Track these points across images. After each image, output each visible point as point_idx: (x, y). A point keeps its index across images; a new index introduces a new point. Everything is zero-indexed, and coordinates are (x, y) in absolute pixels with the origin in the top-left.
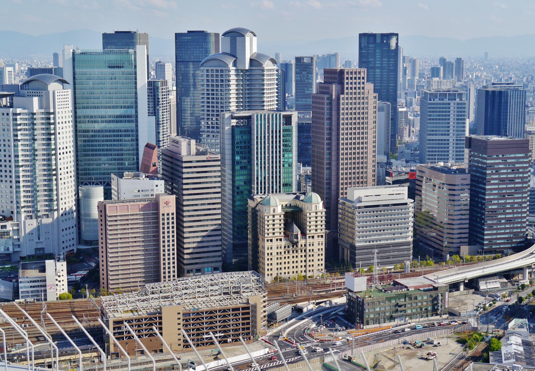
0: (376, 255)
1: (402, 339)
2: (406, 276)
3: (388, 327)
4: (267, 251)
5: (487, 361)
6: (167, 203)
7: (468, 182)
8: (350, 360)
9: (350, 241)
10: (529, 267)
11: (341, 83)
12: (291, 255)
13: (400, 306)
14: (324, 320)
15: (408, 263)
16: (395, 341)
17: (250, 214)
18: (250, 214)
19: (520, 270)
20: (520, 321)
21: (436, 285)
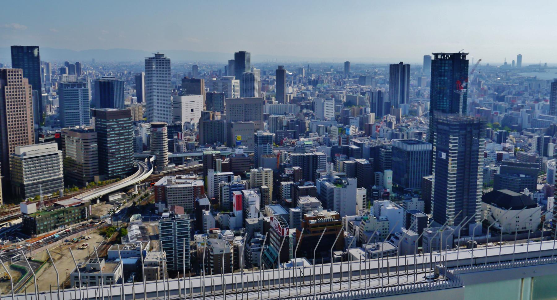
0: (41, 188)
1: (64, 239)
2: (61, 199)
3: (54, 233)
5: (120, 242)
7: (96, 137)
8: (30, 259)
9: (20, 181)
10: (137, 184)
13: (61, 219)
14: (7, 236)
15: (62, 191)
16: (60, 241)
19: (132, 186)
20: (136, 216)
21: (83, 202)
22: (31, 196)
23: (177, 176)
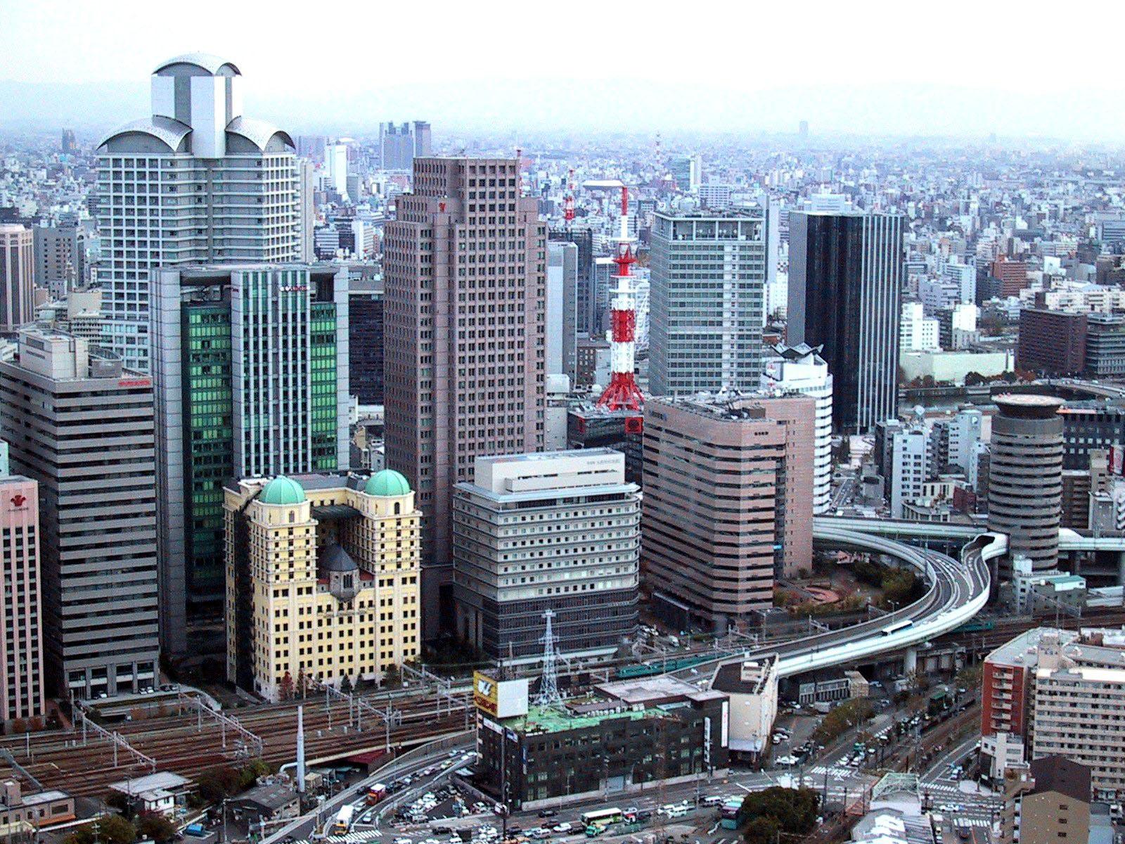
0: (549, 625)
4: (273, 621)
6: (18, 501)
9: (483, 591)
10: (916, 645)
11: (459, 195)
12: (336, 627)
17: (229, 529)
18: (229, 529)
20: (901, 779)
22: (517, 655)
23: (1087, 632)
